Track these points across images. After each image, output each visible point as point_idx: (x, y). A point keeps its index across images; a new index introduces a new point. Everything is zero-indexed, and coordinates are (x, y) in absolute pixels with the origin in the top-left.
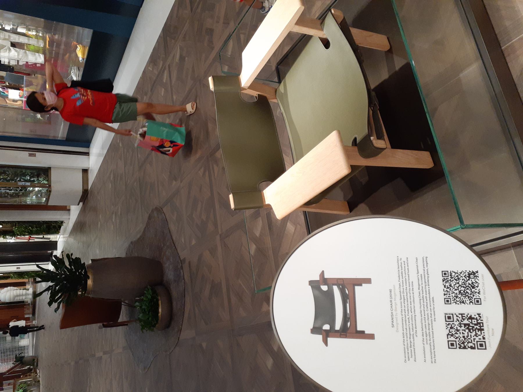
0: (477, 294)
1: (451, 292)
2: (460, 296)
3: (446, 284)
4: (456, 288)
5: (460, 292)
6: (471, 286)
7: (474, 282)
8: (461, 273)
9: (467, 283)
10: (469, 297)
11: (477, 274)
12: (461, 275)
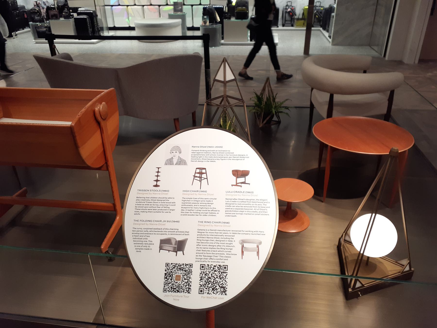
2: (206, 277)
3: (216, 268)
4: (213, 275)
5: (210, 278)
7: (218, 291)
9: (217, 285)
11: (224, 294)
12: (224, 281)
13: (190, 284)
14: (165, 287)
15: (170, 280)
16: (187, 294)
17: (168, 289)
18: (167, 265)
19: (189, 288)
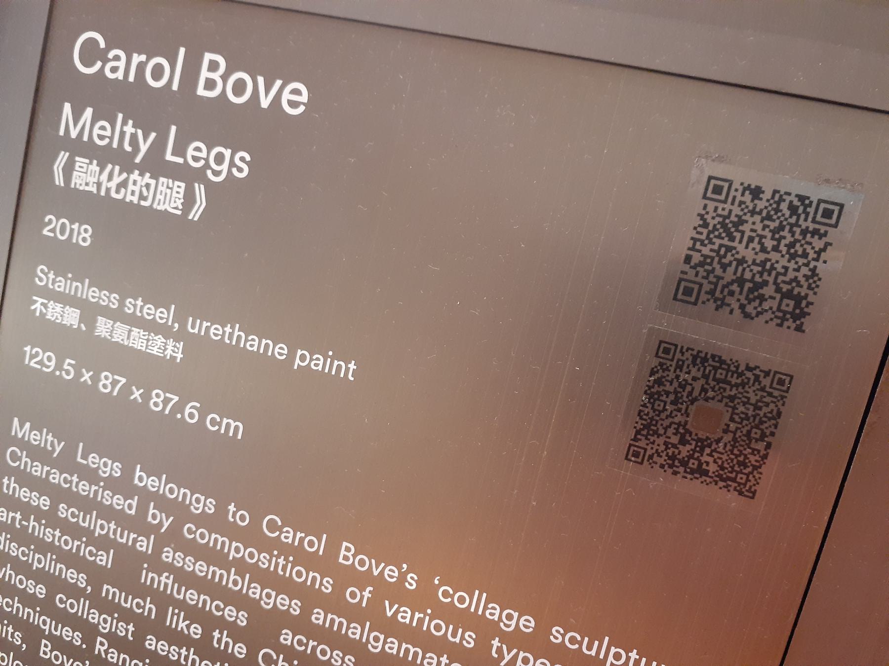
7: (766, 305)
11: (790, 323)
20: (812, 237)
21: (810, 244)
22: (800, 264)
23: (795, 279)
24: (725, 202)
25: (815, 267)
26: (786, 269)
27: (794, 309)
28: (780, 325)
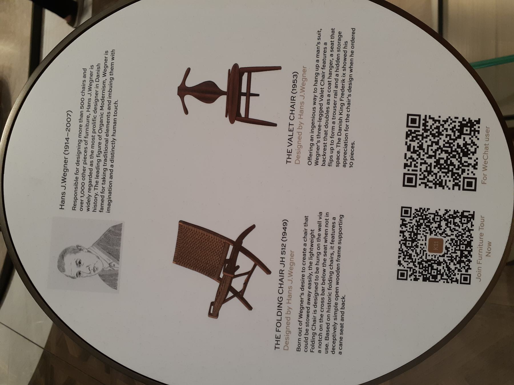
0: (471, 169)
1: (419, 161)
2: (436, 171)
3: (413, 144)
4: (431, 153)
5: (437, 162)
6: (462, 151)
7: (469, 142)
8: (446, 121)
9: (455, 144)
10: (453, 174)
11: (476, 127)
12: (446, 126)
13: (452, 213)
14: (457, 281)
15: (440, 268)
16: (476, 222)
17: (464, 271)
18: (401, 276)
19: (462, 216)
20: (427, 126)
21: (431, 126)
22: (443, 129)
23: (452, 129)
24: (416, 175)
25: (443, 121)
26: (447, 136)
27: (468, 127)
28: (478, 132)
